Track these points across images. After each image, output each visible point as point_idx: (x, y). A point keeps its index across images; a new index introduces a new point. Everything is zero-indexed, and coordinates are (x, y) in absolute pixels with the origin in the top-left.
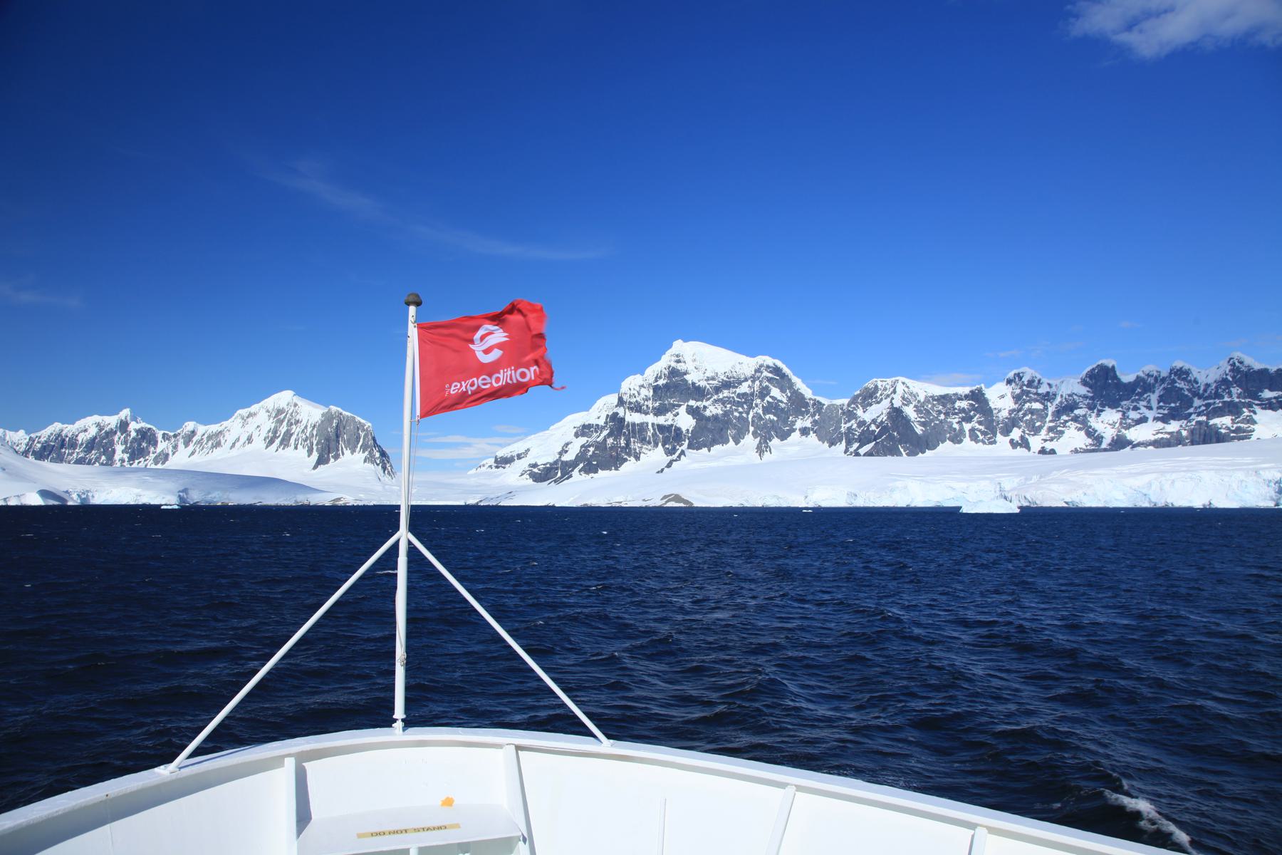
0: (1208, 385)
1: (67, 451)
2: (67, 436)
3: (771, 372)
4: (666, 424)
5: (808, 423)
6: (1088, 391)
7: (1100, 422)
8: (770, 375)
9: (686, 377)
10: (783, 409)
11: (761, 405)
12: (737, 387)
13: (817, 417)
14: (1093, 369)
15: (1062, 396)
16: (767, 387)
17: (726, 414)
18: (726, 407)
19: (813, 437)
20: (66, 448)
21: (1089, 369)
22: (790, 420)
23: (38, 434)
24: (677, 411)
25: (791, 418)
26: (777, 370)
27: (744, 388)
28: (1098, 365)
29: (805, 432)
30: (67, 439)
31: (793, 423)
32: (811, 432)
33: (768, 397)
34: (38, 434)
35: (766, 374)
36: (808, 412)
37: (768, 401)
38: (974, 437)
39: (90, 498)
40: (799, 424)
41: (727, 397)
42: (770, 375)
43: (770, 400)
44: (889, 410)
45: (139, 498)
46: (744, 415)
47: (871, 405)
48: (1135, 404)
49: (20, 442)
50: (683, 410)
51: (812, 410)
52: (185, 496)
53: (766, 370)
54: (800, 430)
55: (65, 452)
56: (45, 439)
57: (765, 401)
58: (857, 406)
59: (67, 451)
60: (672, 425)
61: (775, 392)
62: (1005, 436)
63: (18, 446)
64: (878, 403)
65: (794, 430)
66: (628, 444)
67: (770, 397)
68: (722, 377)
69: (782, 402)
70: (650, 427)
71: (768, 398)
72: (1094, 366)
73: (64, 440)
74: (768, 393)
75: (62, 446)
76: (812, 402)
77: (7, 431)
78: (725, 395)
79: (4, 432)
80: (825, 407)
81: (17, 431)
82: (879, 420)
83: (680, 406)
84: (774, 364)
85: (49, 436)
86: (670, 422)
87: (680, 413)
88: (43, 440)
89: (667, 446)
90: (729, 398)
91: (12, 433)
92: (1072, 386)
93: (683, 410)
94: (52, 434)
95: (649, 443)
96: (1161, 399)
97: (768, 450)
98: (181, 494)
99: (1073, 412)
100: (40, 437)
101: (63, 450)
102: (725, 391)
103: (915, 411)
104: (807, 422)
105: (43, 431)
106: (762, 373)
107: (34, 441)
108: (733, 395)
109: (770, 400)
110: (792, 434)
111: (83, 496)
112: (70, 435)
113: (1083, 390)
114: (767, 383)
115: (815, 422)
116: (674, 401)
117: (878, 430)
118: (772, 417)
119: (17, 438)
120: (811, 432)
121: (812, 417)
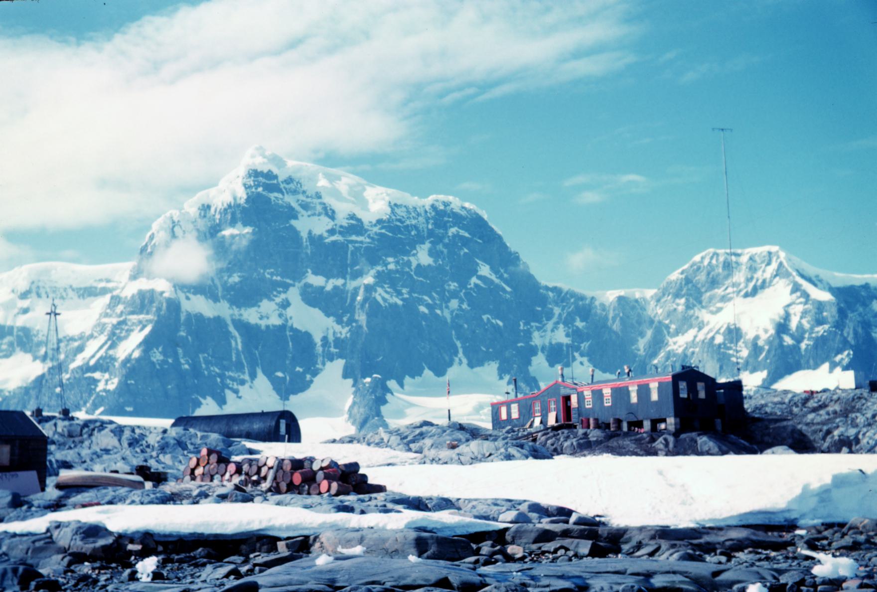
4: (263, 323)
5: (561, 336)
9: (293, 222)
11: (462, 294)
12: (407, 253)
17: (410, 306)
18: (402, 294)
22: (521, 328)
24: (283, 296)
27: (422, 256)
31: (528, 335)
41: (397, 271)
43: (478, 282)
46: (438, 312)
50: (294, 294)
60: (283, 327)
66: (195, 366)
68: (376, 229)
70: (231, 329)
71: (474, 280)
78: (392, 267)
83: (286, 287)
86: (275, 321)
87: (291, 301)
89: (280, 374)
90: (402, 273)
93: (294, 294)
95: (239, 367)
102: (390, 259)
106: (446, 229)
108: (407, 269)
109: (478, 282)
115: (577, 335)
116: (272, 274)
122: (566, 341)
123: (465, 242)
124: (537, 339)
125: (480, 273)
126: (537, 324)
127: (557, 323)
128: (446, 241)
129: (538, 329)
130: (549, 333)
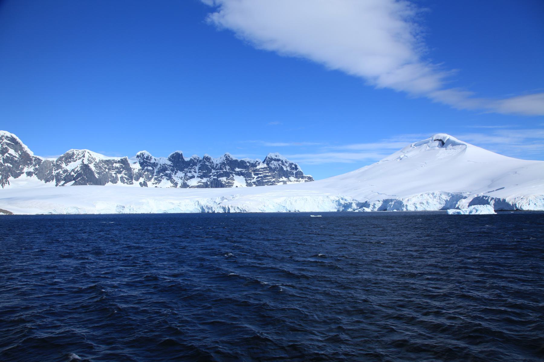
0: (217, 164)
3: (9, 140)
5: (31, 169)
6: (171, 163)
7: (176, 177)
8: (9, 142)
10: (16, 161)
13: (37, 167)
14: (174, 154)
15: (160, 165)
16: (6, 148)
19: (34, 178)
21: (172, 154)
25: (21, 166)
26: (13, 140)
28: (176, 153)
29: (29, 174)
31: (22, 169)
32: (34, 174)
33: (7, 153)
35: (5, 141)
36: (31, 164)
37: (6, 156)
38: (122, 180)
40: (26, 170)
42: (9, 142)
43: (8, 155)
44: (81, 165)
47: (70, 162)
48: (190, 170)
51: (34, 163)
53: (6, 139)
54: (26, 173)
57: (5, 156)
58: (62, 162)
61: (11, 151)
62: (137, 181)
64: (75, 161)
65: (23, 173)
67: (8, 154)
69: (16, 157)
71: (7, 154)
72: (174, 153)
74: (7, 151)
76: (34, 158)
80: (42, 162)
82: (76, 170)
84: (11, 136)
92: (164, 160)
96: (200, 169)
97: (7, 183)
99: (165, 172)
103: (94, 166)
104: (31, 169)
106: (3, 140)
109: (8, 155)
110: (22, 175)
113: (169, 163)
114: (6, 146)
115: (36, 169)
117: (75, 175)
118: (9, 165)
120: (34, 174)
121: (34, 166)
122: (33, 171)
123: (8, 144)
124: (26, 170)
125: (8, 153)
126: (27, 166)
127: (32, 166)
128: (2, 143)
129: (27, 167)
130: (29, 169)
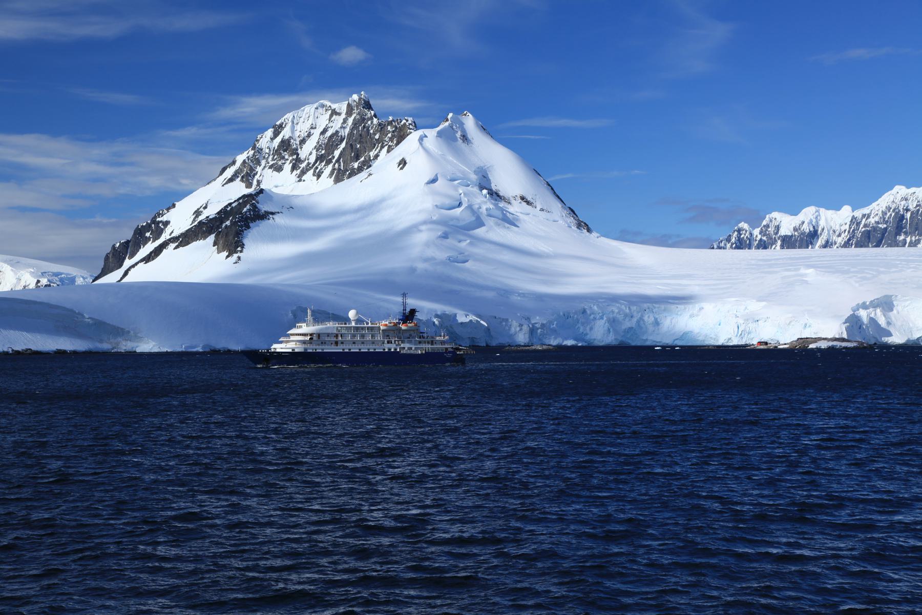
1: (908, 240)
2: (907, 210)
20: (906, 233)
23: (866, 211)
30: (908, 215)
34: (866, 211)
39: (651, 328)
45: (752, 326)
49: (843, 228)
52: (882, 321)
55: (905, 241)
56: (877, 219)
59: (908, 240)
63: (839, 235)
73: (903, 217)
75: (899, 229)
77: (822, 211)
79: (817, 211)
81: (838, 208)
85: (884, 213)
88: (872, 220)
91: (830, 214)
94: (889, 208)
98: (863, 314)
100: (869, 216)
101: (902, 237)
105: (874, 205)
107: (858, 224)
111: (627, 324)
112: (912, 207)
119: (839, 221)
